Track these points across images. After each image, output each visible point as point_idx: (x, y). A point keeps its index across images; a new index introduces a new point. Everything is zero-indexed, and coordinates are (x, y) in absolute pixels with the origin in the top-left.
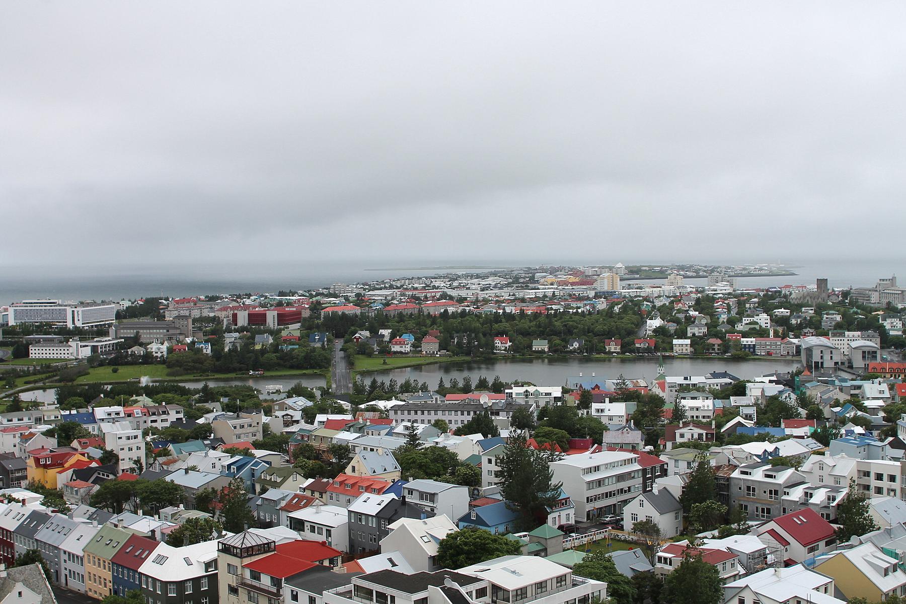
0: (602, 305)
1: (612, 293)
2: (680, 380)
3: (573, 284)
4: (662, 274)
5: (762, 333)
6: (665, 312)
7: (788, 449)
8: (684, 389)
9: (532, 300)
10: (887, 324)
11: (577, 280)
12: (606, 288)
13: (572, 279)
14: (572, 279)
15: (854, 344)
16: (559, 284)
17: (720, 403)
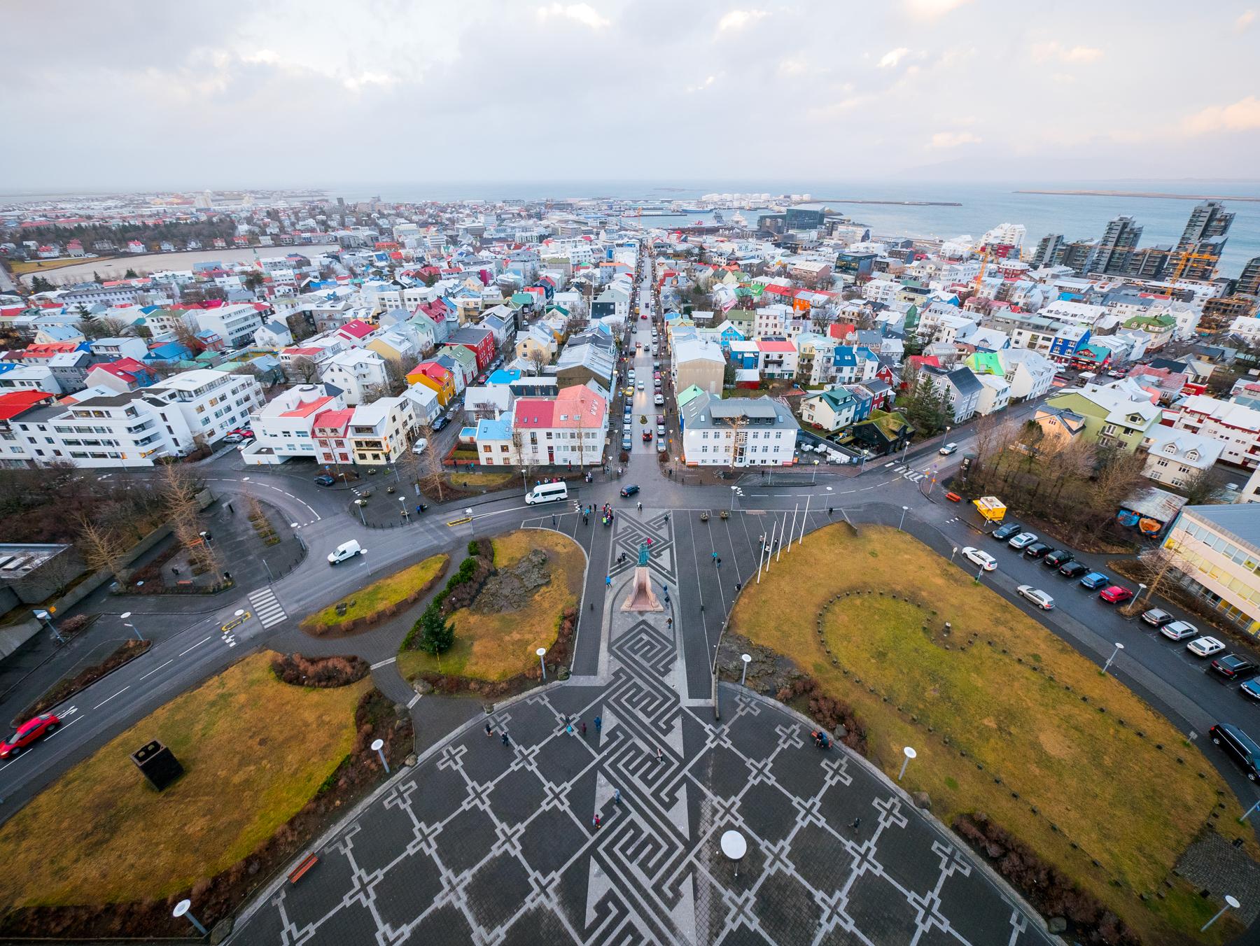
0: (203, 218)
1: (209, 209)
2: (269, 260)
3: (177, 204)
4: (238, 197)
5: (312, 230)
6: (249, 221)
7: (340, 291)
8: (275, 265)
9: (150, 216)
10: (380, 222)
11: (179, 201)
12: (203, 206)
13: (176, 201)
14: (176, 201)
15: (366, 234)
16: (167, 203)
17: (297, 271)
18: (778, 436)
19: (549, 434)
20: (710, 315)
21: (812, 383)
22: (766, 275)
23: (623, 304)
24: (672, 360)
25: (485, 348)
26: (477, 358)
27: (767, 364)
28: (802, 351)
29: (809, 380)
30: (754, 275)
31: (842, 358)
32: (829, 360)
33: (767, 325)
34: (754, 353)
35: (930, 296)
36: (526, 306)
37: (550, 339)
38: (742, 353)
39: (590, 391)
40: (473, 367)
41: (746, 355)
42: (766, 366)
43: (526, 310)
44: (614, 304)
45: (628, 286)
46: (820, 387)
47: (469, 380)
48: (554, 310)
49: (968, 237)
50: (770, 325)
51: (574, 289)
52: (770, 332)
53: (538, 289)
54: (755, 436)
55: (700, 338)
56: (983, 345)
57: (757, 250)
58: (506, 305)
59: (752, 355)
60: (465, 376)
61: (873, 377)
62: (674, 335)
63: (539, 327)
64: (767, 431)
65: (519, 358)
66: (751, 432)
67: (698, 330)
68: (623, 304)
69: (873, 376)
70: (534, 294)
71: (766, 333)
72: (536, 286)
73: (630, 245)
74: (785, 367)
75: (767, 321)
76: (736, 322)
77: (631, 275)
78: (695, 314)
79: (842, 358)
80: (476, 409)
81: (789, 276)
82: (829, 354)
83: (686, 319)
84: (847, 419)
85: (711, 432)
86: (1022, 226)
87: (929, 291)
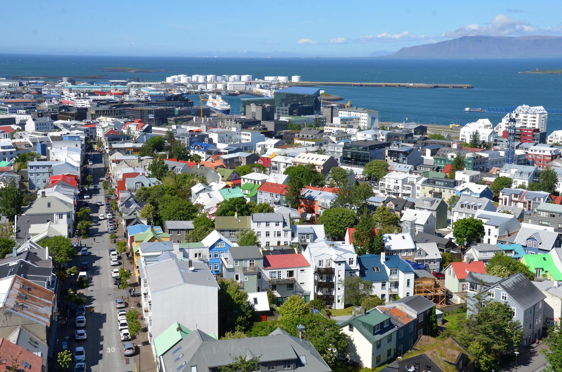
33: (268, 234)
35: (459, 188)
49: (487, 121)
50: (272, 234)
52: (273, 242)
56: (530, 243)
61: (411, 294)
69: (411, 290)
71: (268, 244)
73: (72, 138)
78: (170, 224)
84: (389, 352)
86: (541, 108)
87: (455, 184)
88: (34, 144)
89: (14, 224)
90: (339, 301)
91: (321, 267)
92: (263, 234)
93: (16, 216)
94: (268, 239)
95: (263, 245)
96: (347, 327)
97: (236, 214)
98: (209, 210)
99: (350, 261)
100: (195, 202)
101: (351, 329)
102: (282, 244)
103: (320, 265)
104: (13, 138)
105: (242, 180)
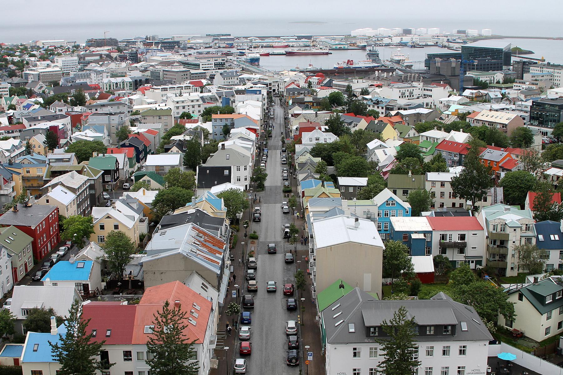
18: (462, 352)
19: (127, 355)
20: (362, 181)
21: (509, 273)
22: (439, 129)
23: (242, 168)
24: (310, 246)
25: (47, 231)
26: (34, 244)
27: (444, 248)
28: (491, 229)
29: (504, 269)
30: (422, 129)
31: (547, 237)
32: (529, 240)
33: (442, 194)
34: (425, 233)
36: (107, 172)
37: (137, 216)
38: (410, 232)
39: (190, 291)
40: (28, 257)
41: (414, 236)
42: (443, 251)
43: (108, 178)
44: (229, 169)
45: (249, 144)
46: (520, 279)
47: (21, 274)
48: (146, 178)
51: (175, 149)
53: (126, 150)
54: (429, 353)
55: (347, 212)
57: (425, 96)
58: (80, 172)
59: (421, 236)
60: (15, 271)
62: (311, 209)
63: (123, 202)
64: (446, 344)
65: (92, 243)
66: (423, 347)
67: (345, 202)
68: (242, 168)
70: (121, 158)
72: (124, 146)
74: (469, 252)
75: (442, 189)
76: (400, 192)
77: (254, 131)
78: (343, 181)
79: (547, 237)
80: (24, 318)
81: (467, 128)
82: (529, 234)
83: (330, 188)
85: (364, 349)
88: (220, 97)
89: (196, 175)
90: (512, 268)
91: (495, 232)
92: (438, 195)
93: (197, 167)
94: (442, 201)
95: (437, 205)
96: (516, 296)
97: (410, 172)
98: (384, 167)
99: (526, 227)
100: (370, 160)
101: (521, 299)
102: (457, 205)
103: (494, 229)
104: (202, 92)
105: (421, 137)
